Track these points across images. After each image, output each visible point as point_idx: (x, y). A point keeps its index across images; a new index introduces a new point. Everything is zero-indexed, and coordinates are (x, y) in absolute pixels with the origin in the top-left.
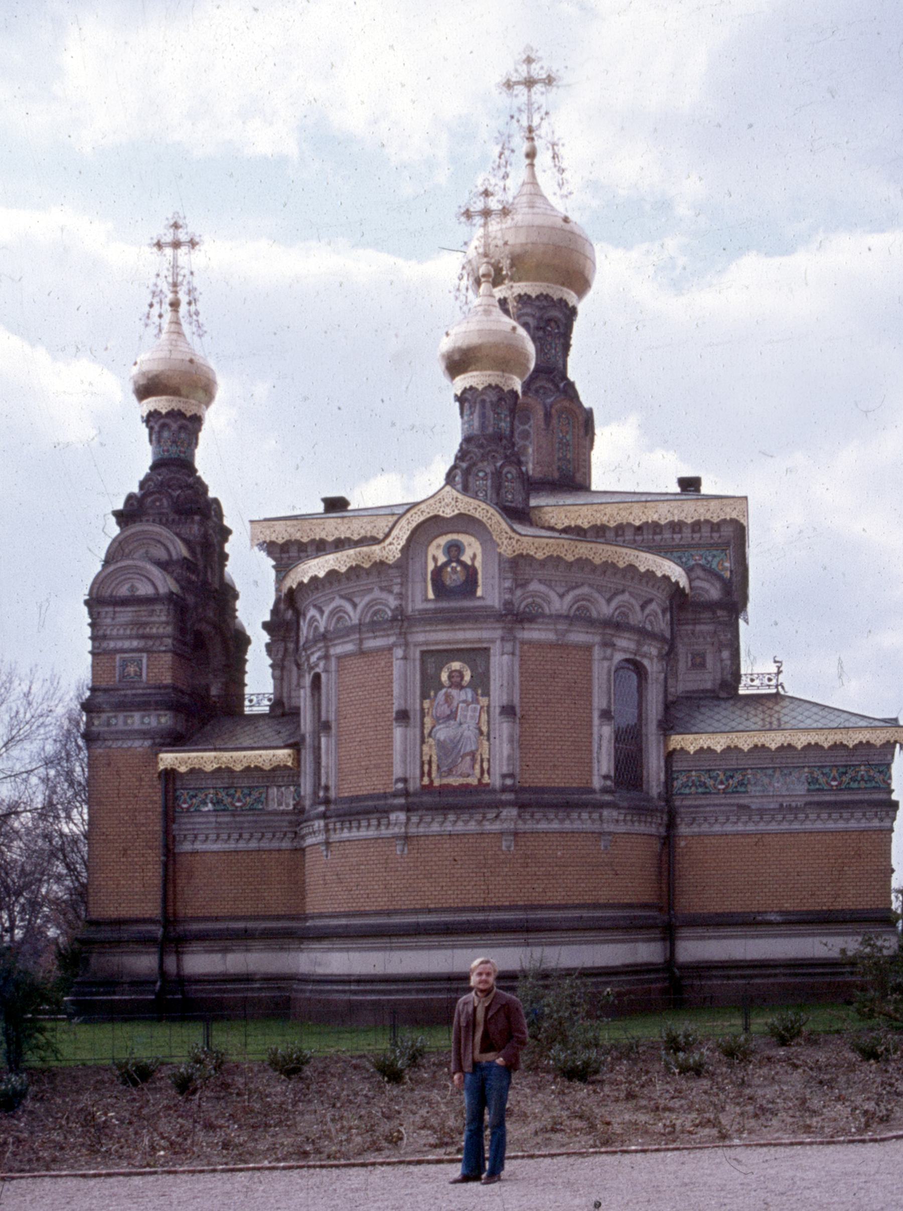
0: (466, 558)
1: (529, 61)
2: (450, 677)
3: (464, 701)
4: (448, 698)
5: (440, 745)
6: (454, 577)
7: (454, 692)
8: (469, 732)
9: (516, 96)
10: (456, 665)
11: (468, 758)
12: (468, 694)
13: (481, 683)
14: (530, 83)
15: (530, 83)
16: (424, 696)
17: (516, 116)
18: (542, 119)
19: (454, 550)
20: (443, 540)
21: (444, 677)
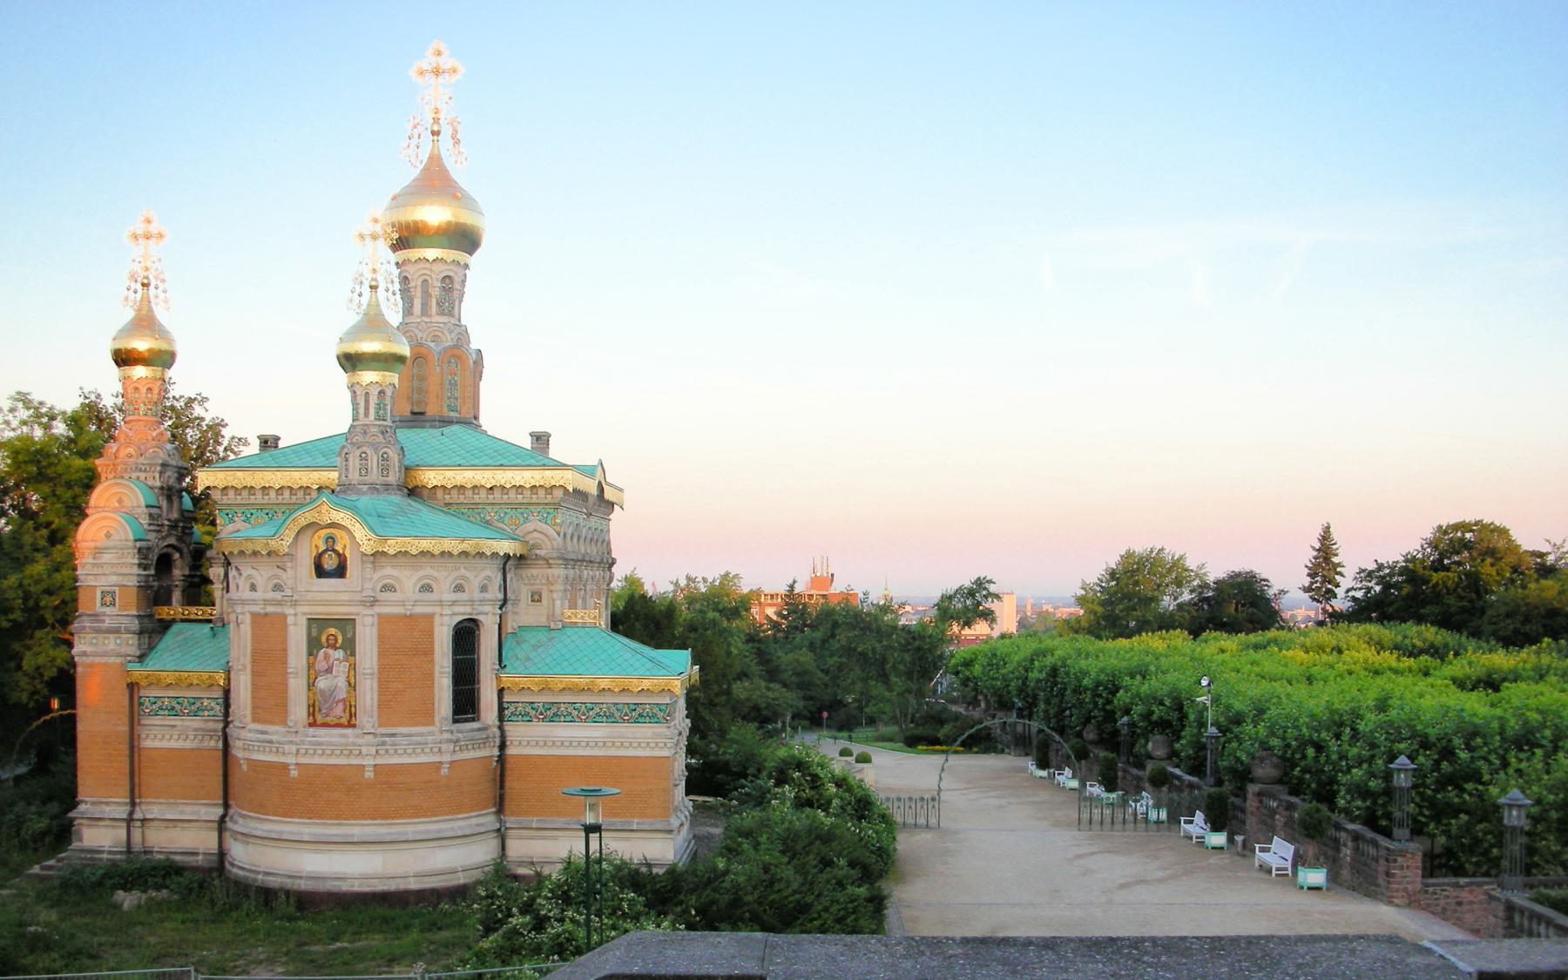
0: (339, 548)
5: (322, 692)
6: (330, 563)
7: (330, 651)
8: (341, 682)
10: (333, 631)
12: (340, 654)
13: (350, 647)
16: (310, 654)
19: (331, 539)
20: (323, 533)
21: (324, 639)
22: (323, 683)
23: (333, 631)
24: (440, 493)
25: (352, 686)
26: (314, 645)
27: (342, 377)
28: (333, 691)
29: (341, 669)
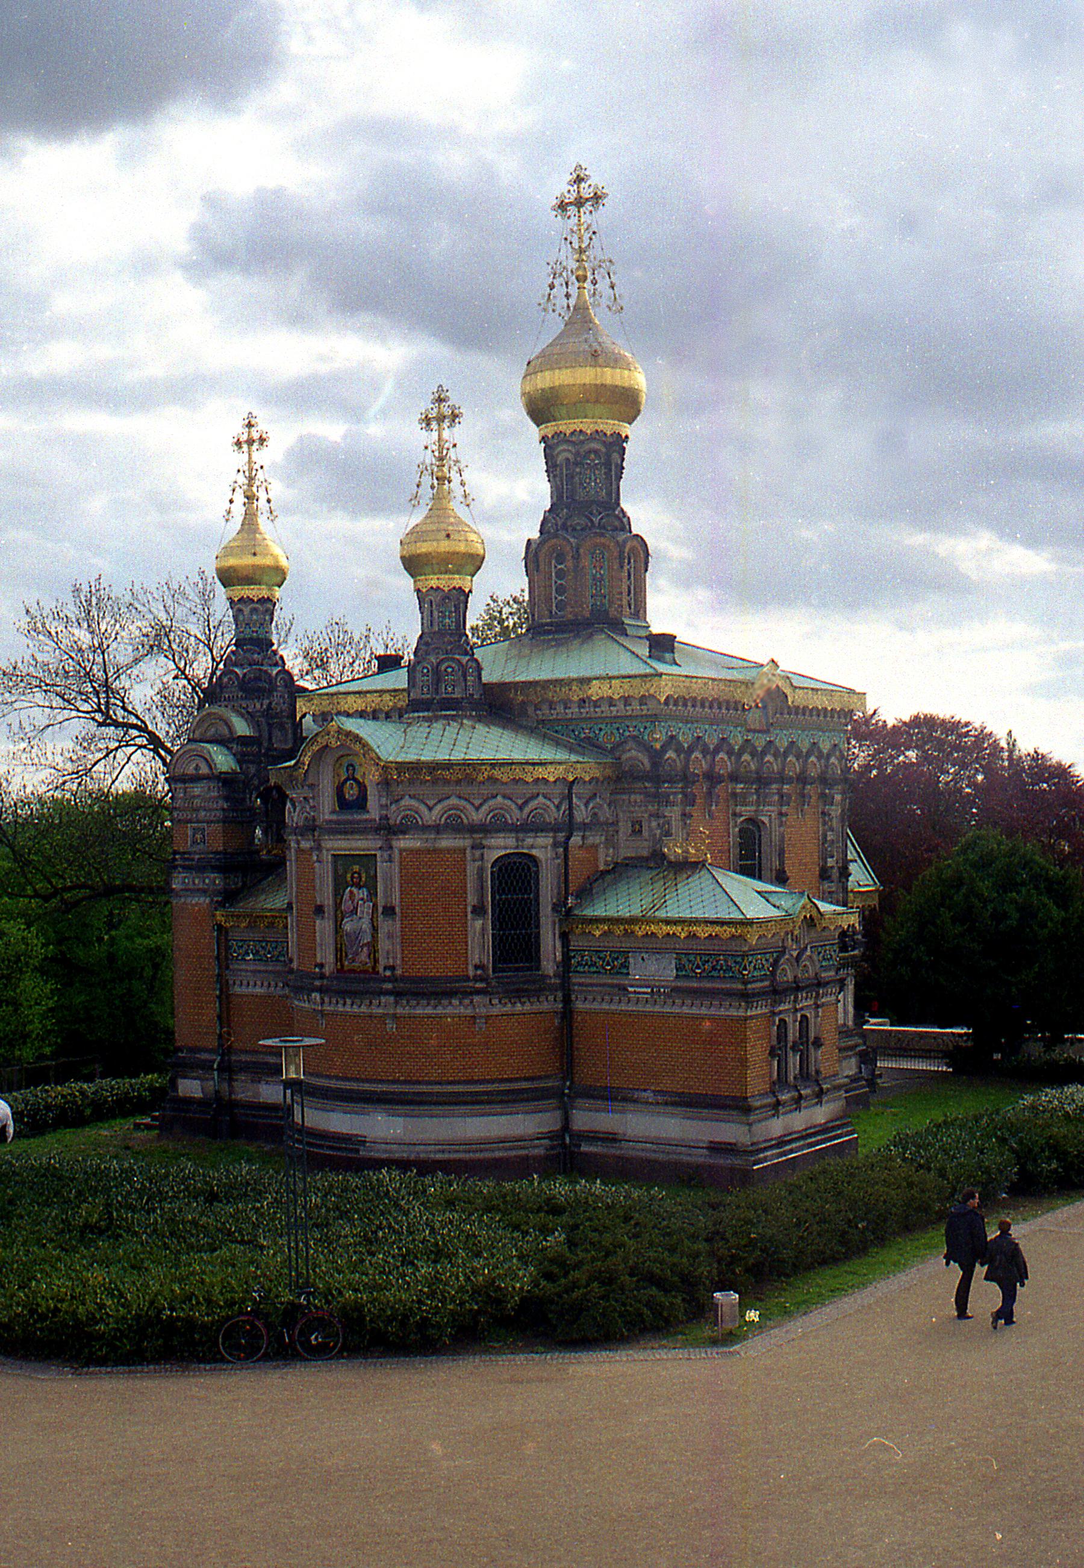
1: (579, 180)
2: (352, 877)
3: (362, 899)
4: (351, 892)
7: (355, 890)
8: (365, 925)
9: (569, 217)
10: (356, 868)
11: (365, 949)
12: (363, 893)
14: (579, 203)
15: (579, 203)
17: (569, 238)
18: (591, 239)
22: (348, 926)
23: (356, 868)
24: (530, 710)
25: (375, 929)
26: (339, 885)
27: (407, 583)
28: (357, 934)
29: (365, 909)
